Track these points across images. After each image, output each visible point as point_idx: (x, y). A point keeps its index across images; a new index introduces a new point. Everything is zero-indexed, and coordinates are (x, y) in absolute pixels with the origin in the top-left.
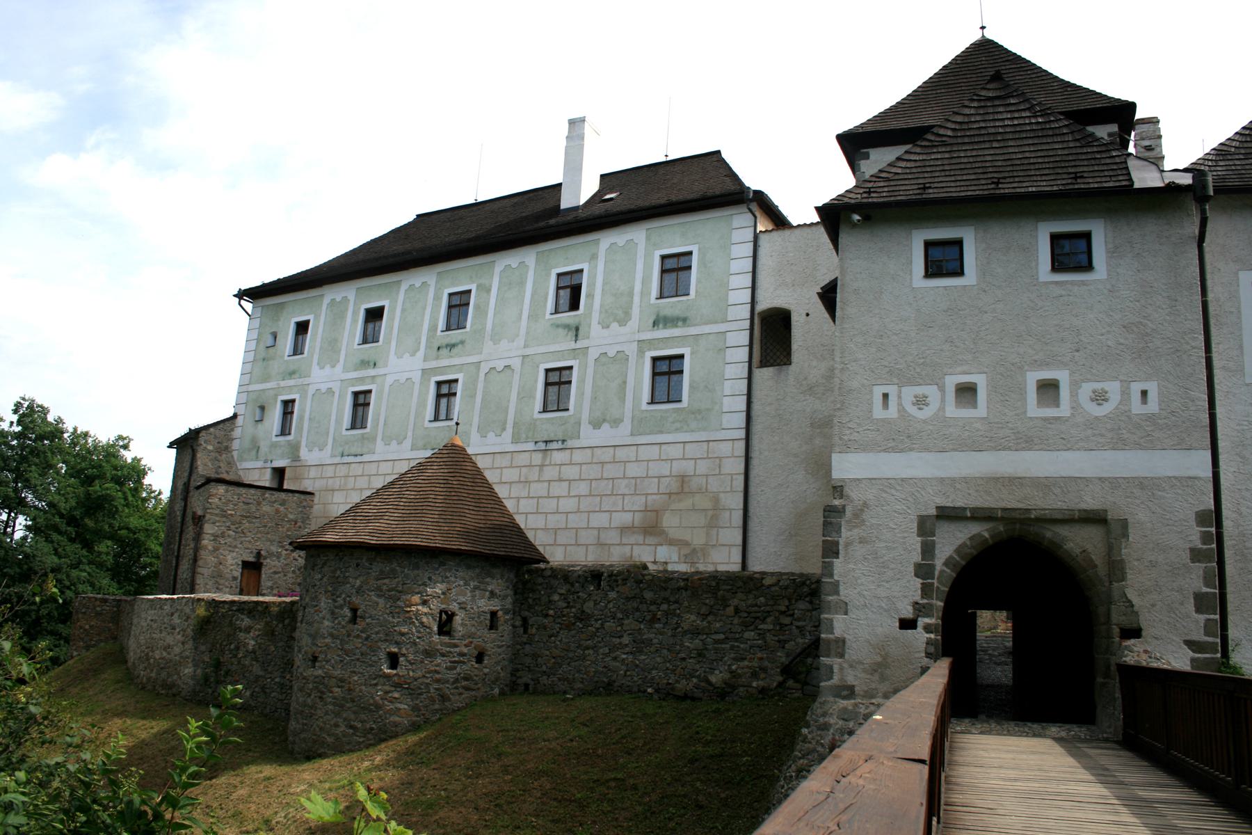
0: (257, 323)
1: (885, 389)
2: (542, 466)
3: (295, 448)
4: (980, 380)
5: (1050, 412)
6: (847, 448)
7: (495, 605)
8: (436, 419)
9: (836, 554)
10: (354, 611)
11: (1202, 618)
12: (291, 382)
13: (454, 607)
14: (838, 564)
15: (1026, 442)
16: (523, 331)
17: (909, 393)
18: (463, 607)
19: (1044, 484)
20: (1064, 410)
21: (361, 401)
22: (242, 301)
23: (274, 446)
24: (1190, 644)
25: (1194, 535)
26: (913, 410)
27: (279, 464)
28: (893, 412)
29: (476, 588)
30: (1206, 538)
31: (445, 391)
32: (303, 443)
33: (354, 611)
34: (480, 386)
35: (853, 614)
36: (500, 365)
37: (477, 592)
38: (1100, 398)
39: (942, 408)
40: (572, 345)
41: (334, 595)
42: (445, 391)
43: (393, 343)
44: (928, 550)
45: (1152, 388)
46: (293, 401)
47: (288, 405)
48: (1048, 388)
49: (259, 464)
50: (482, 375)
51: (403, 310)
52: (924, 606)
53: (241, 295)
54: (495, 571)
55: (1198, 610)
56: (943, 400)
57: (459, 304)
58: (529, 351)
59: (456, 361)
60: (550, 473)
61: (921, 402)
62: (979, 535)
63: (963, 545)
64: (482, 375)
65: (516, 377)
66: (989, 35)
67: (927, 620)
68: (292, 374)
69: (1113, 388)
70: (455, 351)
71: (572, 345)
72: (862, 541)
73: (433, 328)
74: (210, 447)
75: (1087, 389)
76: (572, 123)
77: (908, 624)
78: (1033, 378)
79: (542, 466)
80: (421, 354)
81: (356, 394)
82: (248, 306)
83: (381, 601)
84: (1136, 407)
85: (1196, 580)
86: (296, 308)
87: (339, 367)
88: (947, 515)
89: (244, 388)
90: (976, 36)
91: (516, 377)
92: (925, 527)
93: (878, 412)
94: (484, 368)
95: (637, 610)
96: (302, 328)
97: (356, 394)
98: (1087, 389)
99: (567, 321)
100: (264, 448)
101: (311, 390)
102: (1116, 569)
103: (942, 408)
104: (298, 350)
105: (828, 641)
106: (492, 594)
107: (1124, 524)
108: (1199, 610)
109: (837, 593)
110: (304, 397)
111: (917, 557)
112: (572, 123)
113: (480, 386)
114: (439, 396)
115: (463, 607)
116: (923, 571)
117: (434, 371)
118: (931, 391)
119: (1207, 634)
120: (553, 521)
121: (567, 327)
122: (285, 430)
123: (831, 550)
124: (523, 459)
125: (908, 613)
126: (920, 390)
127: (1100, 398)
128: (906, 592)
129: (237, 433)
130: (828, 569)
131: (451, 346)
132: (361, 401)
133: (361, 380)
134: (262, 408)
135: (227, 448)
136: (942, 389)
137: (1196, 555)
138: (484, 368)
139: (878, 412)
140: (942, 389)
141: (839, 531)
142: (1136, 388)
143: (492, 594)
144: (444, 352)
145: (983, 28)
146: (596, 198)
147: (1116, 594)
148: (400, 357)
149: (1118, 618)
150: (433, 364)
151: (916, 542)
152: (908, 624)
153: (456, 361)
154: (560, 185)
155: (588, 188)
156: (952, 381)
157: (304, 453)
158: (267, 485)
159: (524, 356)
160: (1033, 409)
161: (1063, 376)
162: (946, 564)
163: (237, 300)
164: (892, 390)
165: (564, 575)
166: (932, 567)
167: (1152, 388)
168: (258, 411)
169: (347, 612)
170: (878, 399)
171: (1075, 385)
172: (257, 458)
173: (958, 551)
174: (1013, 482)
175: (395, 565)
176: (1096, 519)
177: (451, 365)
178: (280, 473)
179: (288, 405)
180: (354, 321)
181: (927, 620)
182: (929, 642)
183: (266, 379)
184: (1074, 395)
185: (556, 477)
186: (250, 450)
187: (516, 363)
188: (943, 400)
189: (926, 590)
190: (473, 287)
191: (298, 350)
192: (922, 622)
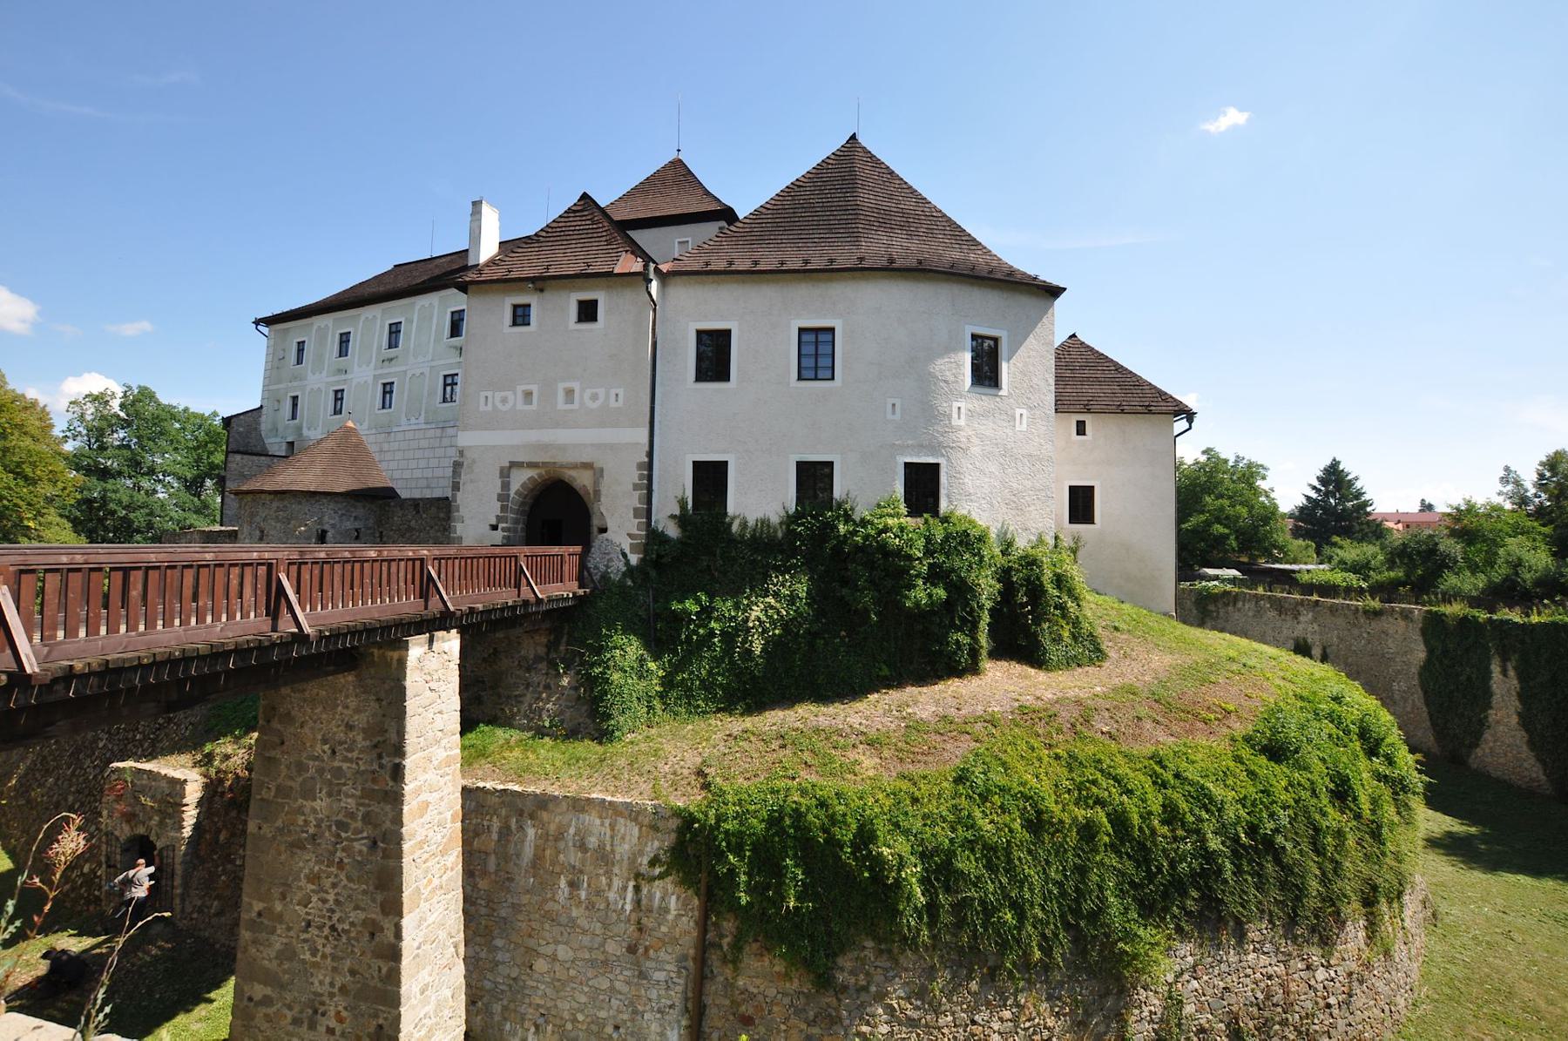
0: (272, 342)
1: (486, 393)
2: (441, 437)
3: (300, 428)
4: (534, 388)
5: (569, 407)
6: (465, 429)
7: (357, 525)
8: (383, 407)
9: (459, 490)
10: (262, 532)
11: (637, 520)
12: (295, 384)
13: (326, 527)
14: (459, 495)
15: (557, 425)
16: (431, 351)
17: (498, 395)
18: (333, 526)
19: (563, 448)
20: (576, 406)
21: (339, 396)
22: (259, 327)
23: (287, 427)
24: (630, 535)
25: (634, 476)
26: (499, 406)
27: (290, 440)
28: (490, 407)
29: (343, 515)
30: (641, 477)
31: (388, 389)
32: (304, 425)
33: (262, 532)
34: (407, 387)
35: (467, 521)
36: (418, 372)
37: (344, 517)
38: (594, 397)
39: (515, 405)
40: (458, 360)
41: (251, 523)
42: (388, 389)
43: (356, 357)
44: (506, 486)
45: (621, 392)
46: (297, 397)
47: (295, 399)
48: (570, 393)
49: (278, 440)
50: (408, 379)
51: (362, 335)
52: (502, 517)
53: (257, 322)
54: (359, 504)
55: (635, 517)
56: (515, 399)
57: (395, 330)
58: (433, 364)
59: (393, 370)
60: (446, 442)
61: (504, 401)
62: (532, 477)
63: (525, 483)
64: (408, 379)
65: (427, 380)
66: (680, 157)
67: (504, 525)
68: (295, 378)
69: (601, 392)
70: (393, 362)
71: (458, 360)
72: (472, 481)
73: (380, 347)
74: (241, 429)
75: (588, 393)
76: (474, 203)
77: (494, 528)
78: (561, 386)
79: (441, 437)
80: (372, 365)
81: (336, 392)
82: (265, 330)
83: (279, 525)
84: (613, 404)
85: (635, 500)
86: (297, 332)
87: (324, 373)
88: (513, 465)
89: (266, 388)
90: (672, 156)
91: (427, 380)
92: (505, 474)
93: (482, 408)
94: (409, 374)
95: (436, 525)
96: (301, 347)
97: (336, 392)
98: (588, 393)
99: (455, 344)
100: (281, 429)
101: (308, 389)
102: (597, 493)
103: (515, 405)
104: (299, 361)
105: (454, 538)
106: (356, 518)
107: (602, 470)
108: (635, 517)
109: (458, 511)
110: (303, 394)
111: (499, 491)
112: (474, 203)
113: (407, 387)
114: (385, 393)
115: (333, 526)
116: (503, 498)
117: (381, 376)
118: (509, 394)
119: (638, 530)
120: (407, 475)
121: (456, 348)
122: (294, 417)
123: (456, 487)
124: (431, 433)
125: (494, 522)
126: (503, 394)
127: (594, 397)
128: (493, 509)
129: (263, 418)
130: (454, 496)
131: (392, 359)
132: (339, 396)
133: (338, 382)
134: (278, 401)
135: (256, 429)
136: (515, 394)
137: (636, 487)
138: (409, 374)
139: (482, 408)
140: (515, 394)
141: (460, 476)
142: (613, 392)
143: (356, 518)
144: (386, 363)
145: (679, 150)
146: (492, 262)
147: (595, 510)
148: (360, 366)
149: (596, 522)
150: (380, 372)
151: (499, 483)
152: (494, 528)
153: (393, 370)
154: (467, 250)
155: (488, 249)
156: (520, 388)
157: (305, 432)
158: (284, 454)
159: (432, 367)
160: (561, 404)
161: (576, 386)
162: (516, 493)
163: (254, 326)
164: (489, 394)
165: (416, 504)
166: (509, 495)
167: (621, 392)
168: (276, 403)
169: (258, 533)
170: (482, 400)
171: (583, 390)
172: (276, 436)
173: (522, 486)
174: (545, 447)
175: (286, 503)
176: (587, 466)
177: (391, 373)
178: (291, 444)
179: (295, 399)
180: (333, 342)
181: (504, 525)
182: (504, 537)
183: (280, 382)
184: (581, 397)
185: (449, 444)
186: (271, 430)
187: (427, 371)
188: (515, 399)
189: (504, 508)
190: (402, 319)
191: (299, 361)
192: (501, 526)
